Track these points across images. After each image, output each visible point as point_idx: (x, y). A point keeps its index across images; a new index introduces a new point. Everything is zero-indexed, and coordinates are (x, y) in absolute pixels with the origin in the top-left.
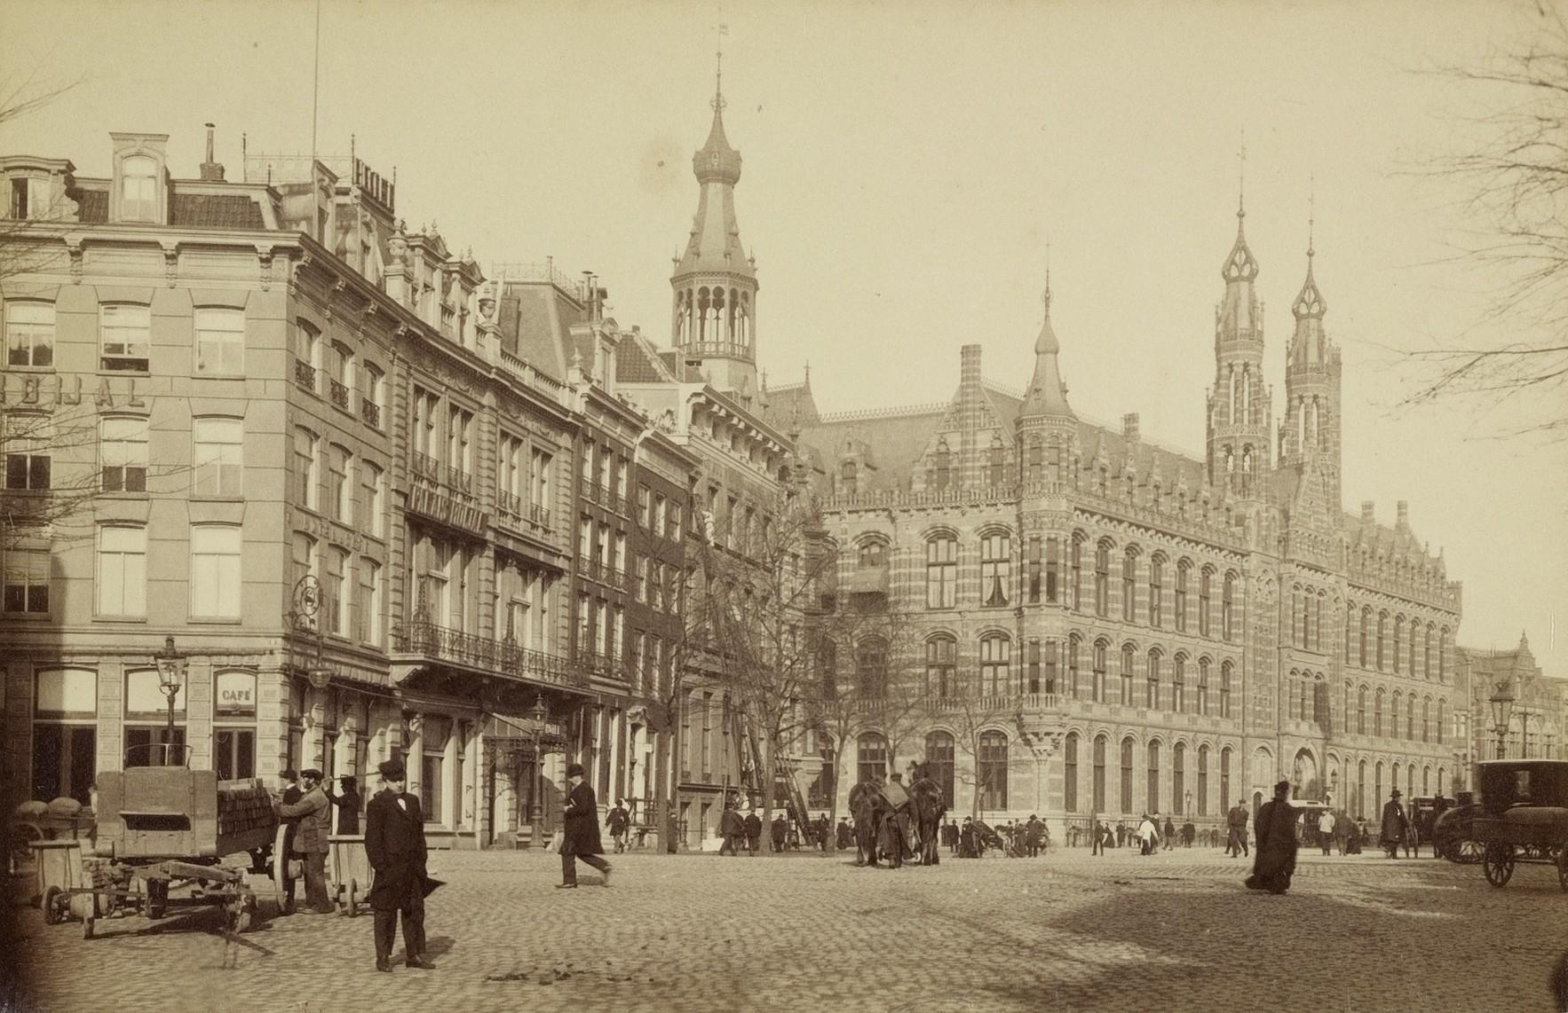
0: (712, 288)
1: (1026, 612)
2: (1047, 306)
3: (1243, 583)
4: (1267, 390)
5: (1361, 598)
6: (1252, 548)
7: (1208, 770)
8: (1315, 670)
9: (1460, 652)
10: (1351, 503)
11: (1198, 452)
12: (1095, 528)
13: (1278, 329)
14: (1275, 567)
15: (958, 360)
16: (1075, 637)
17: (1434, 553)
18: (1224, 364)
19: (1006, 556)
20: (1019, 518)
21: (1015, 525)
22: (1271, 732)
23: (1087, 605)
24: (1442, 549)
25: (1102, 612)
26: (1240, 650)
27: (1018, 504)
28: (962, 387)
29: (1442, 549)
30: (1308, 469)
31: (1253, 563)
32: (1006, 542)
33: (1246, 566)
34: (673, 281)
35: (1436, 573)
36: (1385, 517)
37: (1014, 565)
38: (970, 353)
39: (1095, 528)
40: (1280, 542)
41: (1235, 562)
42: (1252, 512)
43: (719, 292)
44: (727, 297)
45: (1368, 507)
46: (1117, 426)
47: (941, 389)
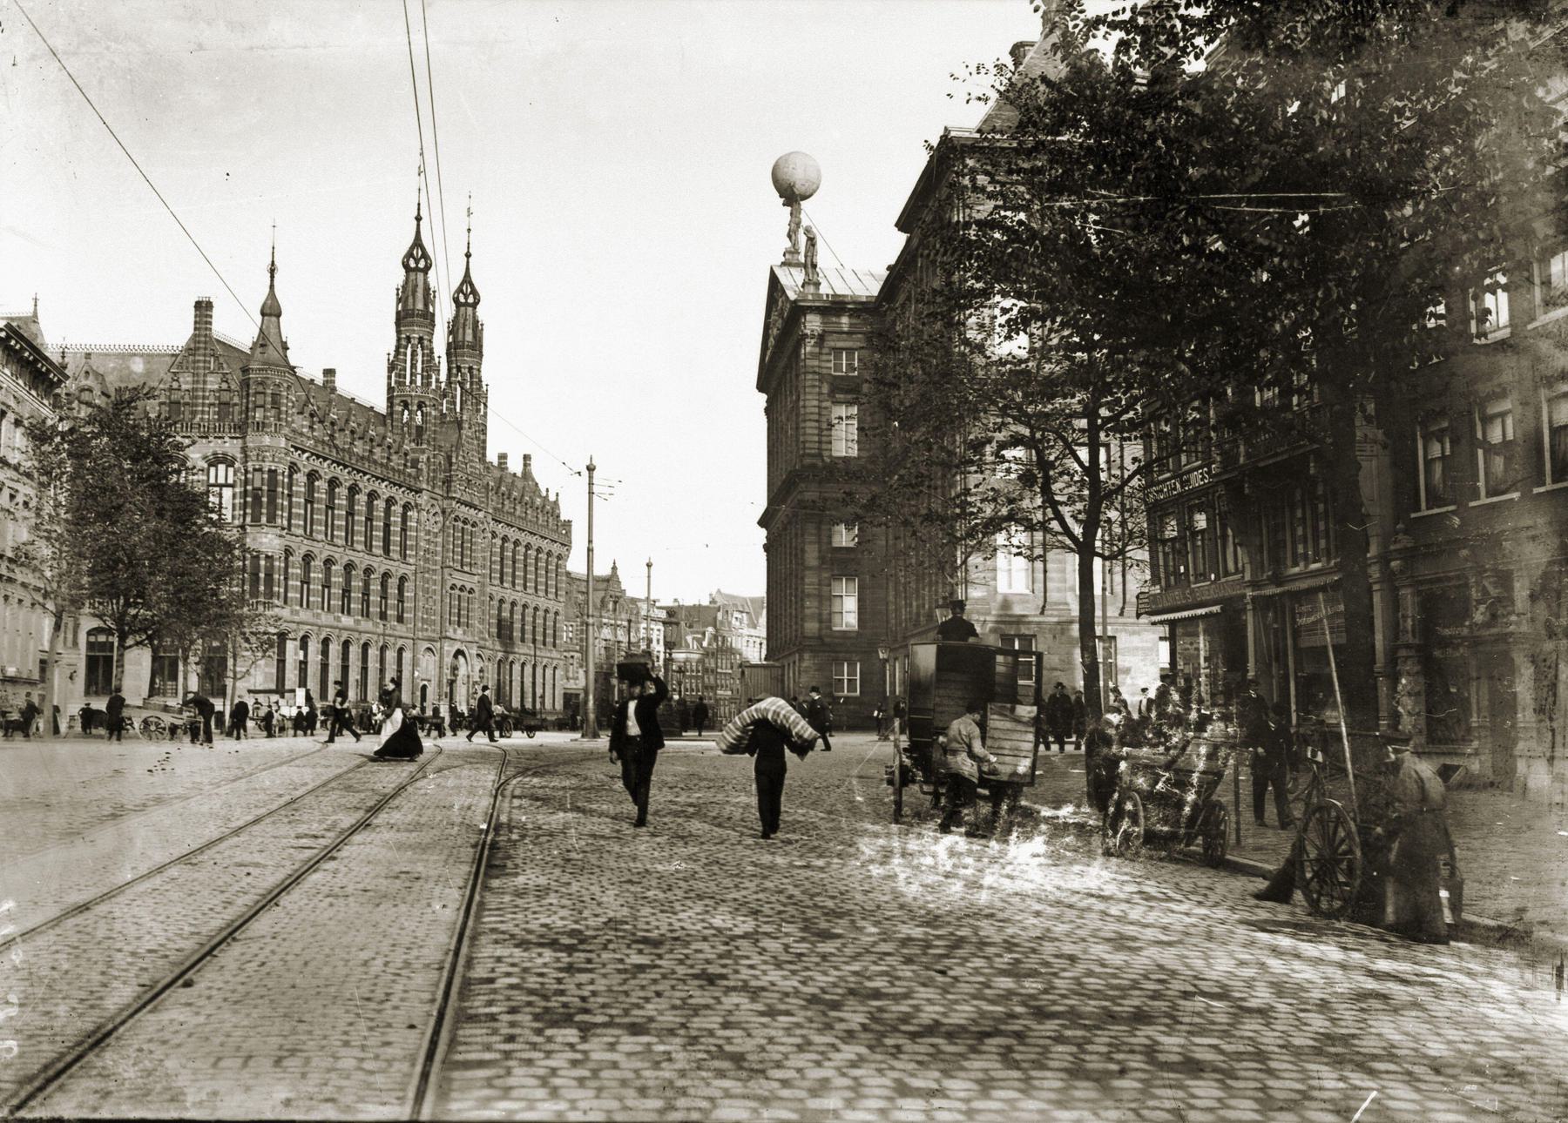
1: (249, 529)
5: (501, 530)
8: (468, 586)
9: (568, 574)
10: (492, 456)
11: (381, 406)
12: (305, 463)
13: (444, 311)
15: (192, 311)
16: (288, 552)
17: (552, 498)
19: (230, 481)
20: (244, 450)
21: (239, 456)
22: (436, 636)
23: (319, 532)
25: (349, 541)
27: (244, 438)
28: (195, 335)
30: (466, 425)
31: (423, 499)
32: (231, 470)
33: (419, 501)
37: (238, 490)
38: (203, 308)
39: (305, 463)
41: (410, 497)
42: (424, 457)
45: (503, 457)
46: (320, 379)
47: (177, 333)
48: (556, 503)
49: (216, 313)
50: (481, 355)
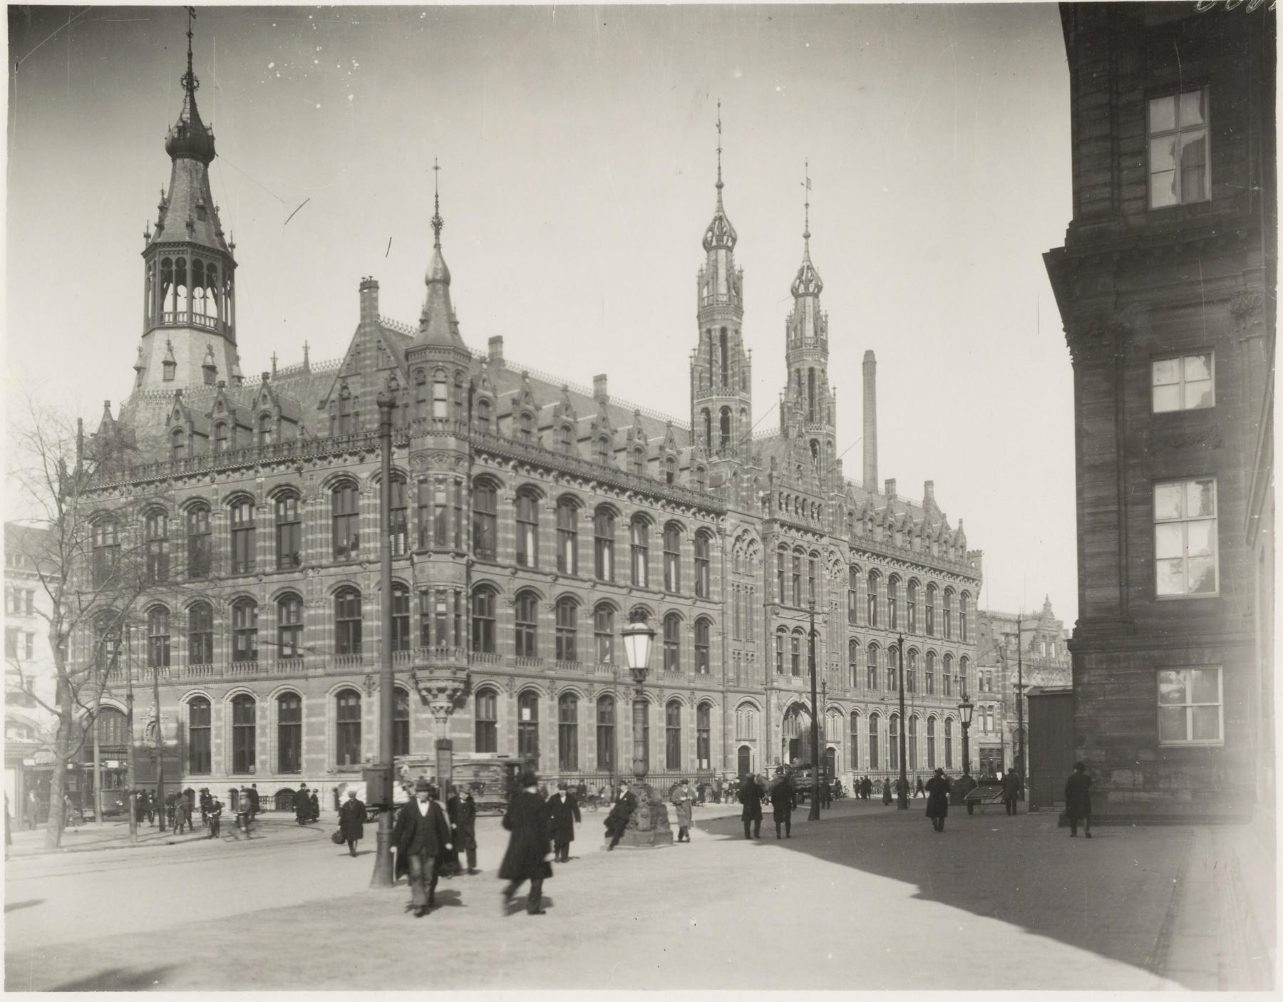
0: (174, 258)
2: (437, 233)
3: (720, 542)
4: (747, 354)
6: (730, 506)
7: (682, 725)
14: (759, 527)
17: (954, 526)
18: (704, 330)
24: (961, 522)
26: (719, 607)
29: (961, 522)
31: (729, 523)
34: (145, 254)
35: (957, 541)
36: (910, 492)
40: (764, 503)
41: (708, 521)
43: (182, 263)
44: (188, 267)
46: (587, 387)
48: (960, 530)
49: (383, 295)
50: (825, 352)
